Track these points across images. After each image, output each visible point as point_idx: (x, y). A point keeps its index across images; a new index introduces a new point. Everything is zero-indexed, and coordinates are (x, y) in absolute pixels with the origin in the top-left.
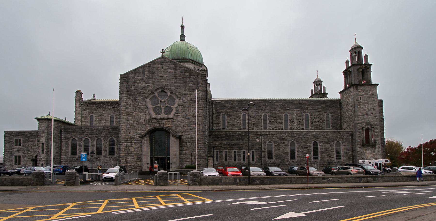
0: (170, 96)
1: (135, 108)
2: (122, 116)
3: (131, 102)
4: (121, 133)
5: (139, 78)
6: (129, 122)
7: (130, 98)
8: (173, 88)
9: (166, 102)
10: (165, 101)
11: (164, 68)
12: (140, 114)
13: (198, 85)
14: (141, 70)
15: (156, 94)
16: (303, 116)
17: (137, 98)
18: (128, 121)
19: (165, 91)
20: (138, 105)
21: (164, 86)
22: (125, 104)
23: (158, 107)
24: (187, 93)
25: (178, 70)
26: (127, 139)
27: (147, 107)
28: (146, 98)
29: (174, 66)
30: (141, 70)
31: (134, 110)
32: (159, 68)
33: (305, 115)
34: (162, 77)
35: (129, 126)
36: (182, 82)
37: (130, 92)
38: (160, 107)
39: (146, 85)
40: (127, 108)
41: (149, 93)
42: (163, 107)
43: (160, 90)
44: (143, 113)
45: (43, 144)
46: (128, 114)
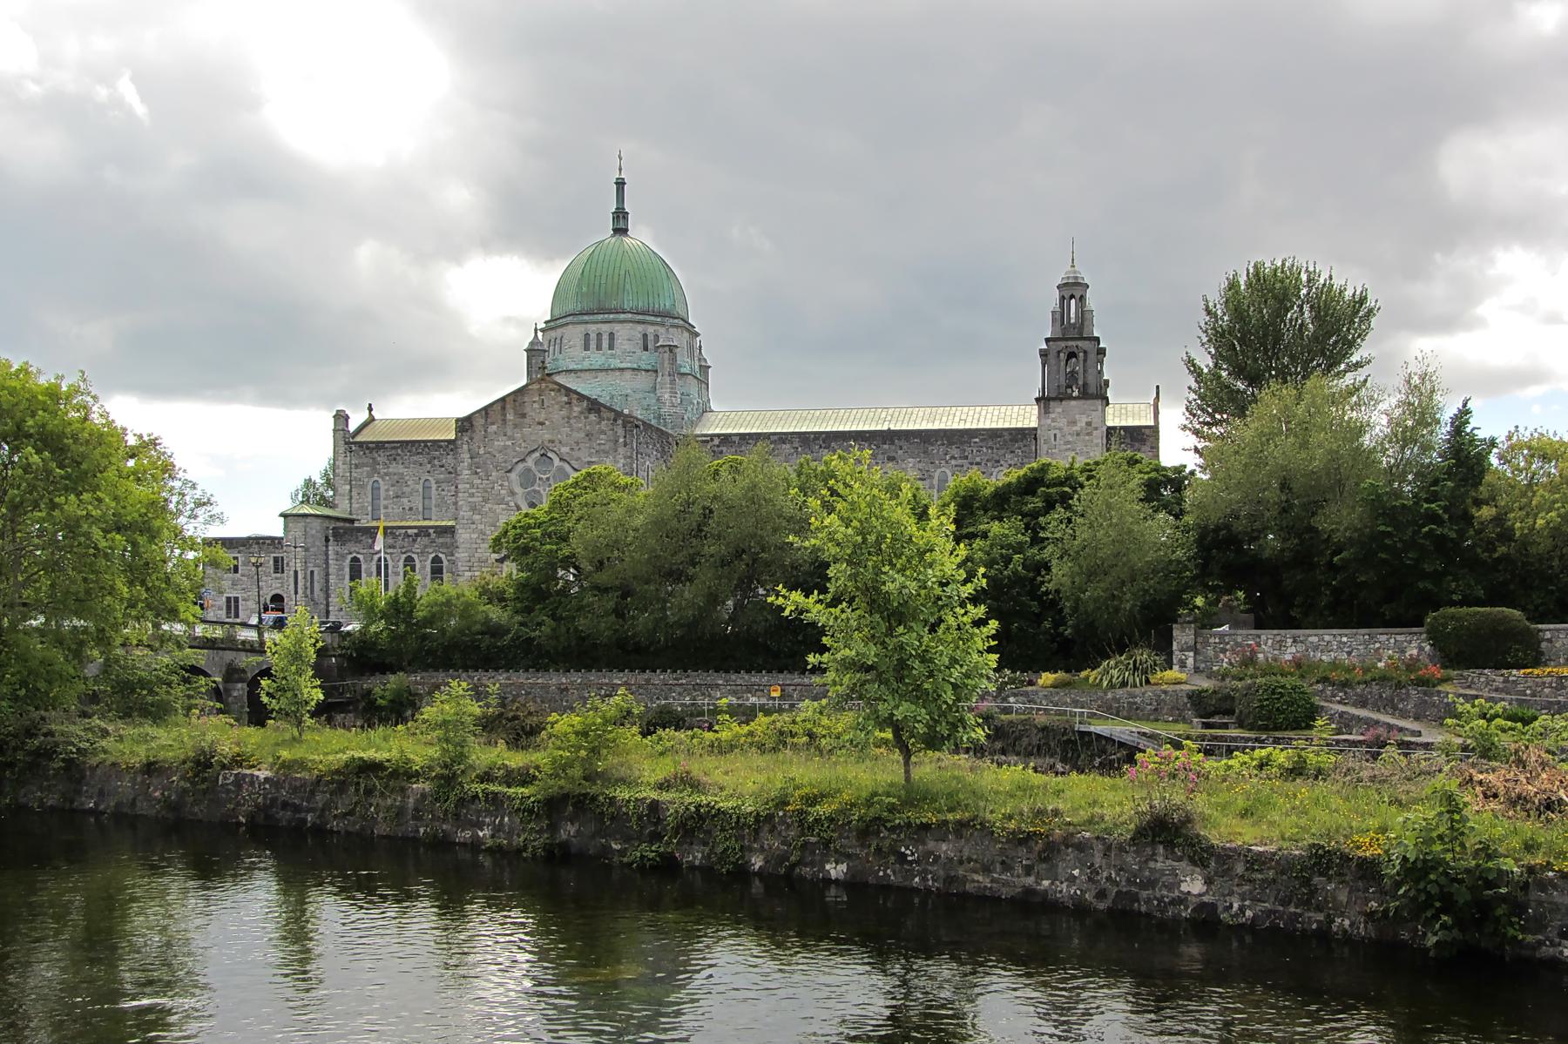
0: (560, 469)
1: (486, 495)
2: (462, 513)
3: (479, 481)
4: (460, 550)
5: (494, 427)
6: (474, 526)
7: (476, 473)
8: (565, 450)
9: (551, 479)
10: (548, 479)
11: (546, 404)
12: (498, 508)
13: (617, 441)
14: (498, 407)
15: (530, 462)
16: (931, 477)
17: (492, 471)
18: (473, 523)
19: (550, 454)
20: (493, 488)
21: (546, 443)
22: (468, 486)
23: (535, 491)
24: (593, 460)
25: (576, 409)
26: (471, 564)
27: (512, 493)
28: (510, 471)
29: (565, 399)
30: (498, 407)
31: (486, 500)
32: (535, 405)
33: (936, 475)
34: (542, 424)
35: (475, 536)
36: (583, 435)
37: (477, 460)
38: (539, 492)
39: (509, 443)
40: (472, 495)
41: (515, 460)
42: (544, 490)
43: (537, 454)
44: (504, 506)
45: (296, 572)
46: (474, 509)
